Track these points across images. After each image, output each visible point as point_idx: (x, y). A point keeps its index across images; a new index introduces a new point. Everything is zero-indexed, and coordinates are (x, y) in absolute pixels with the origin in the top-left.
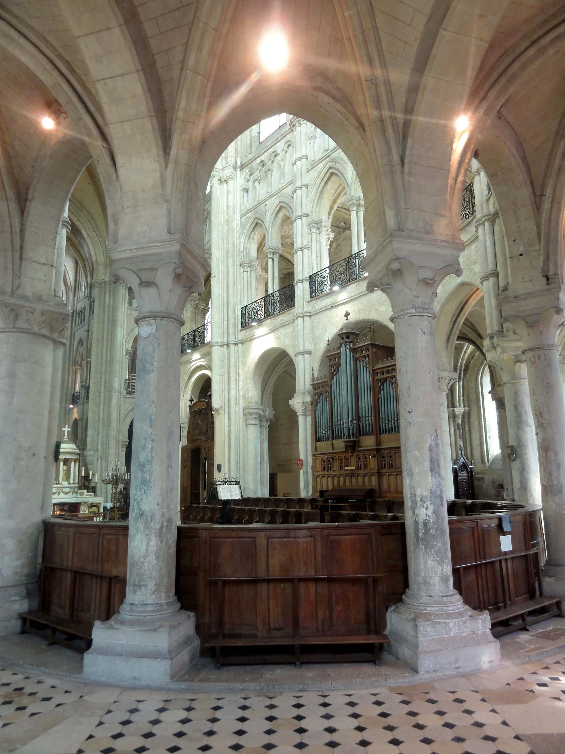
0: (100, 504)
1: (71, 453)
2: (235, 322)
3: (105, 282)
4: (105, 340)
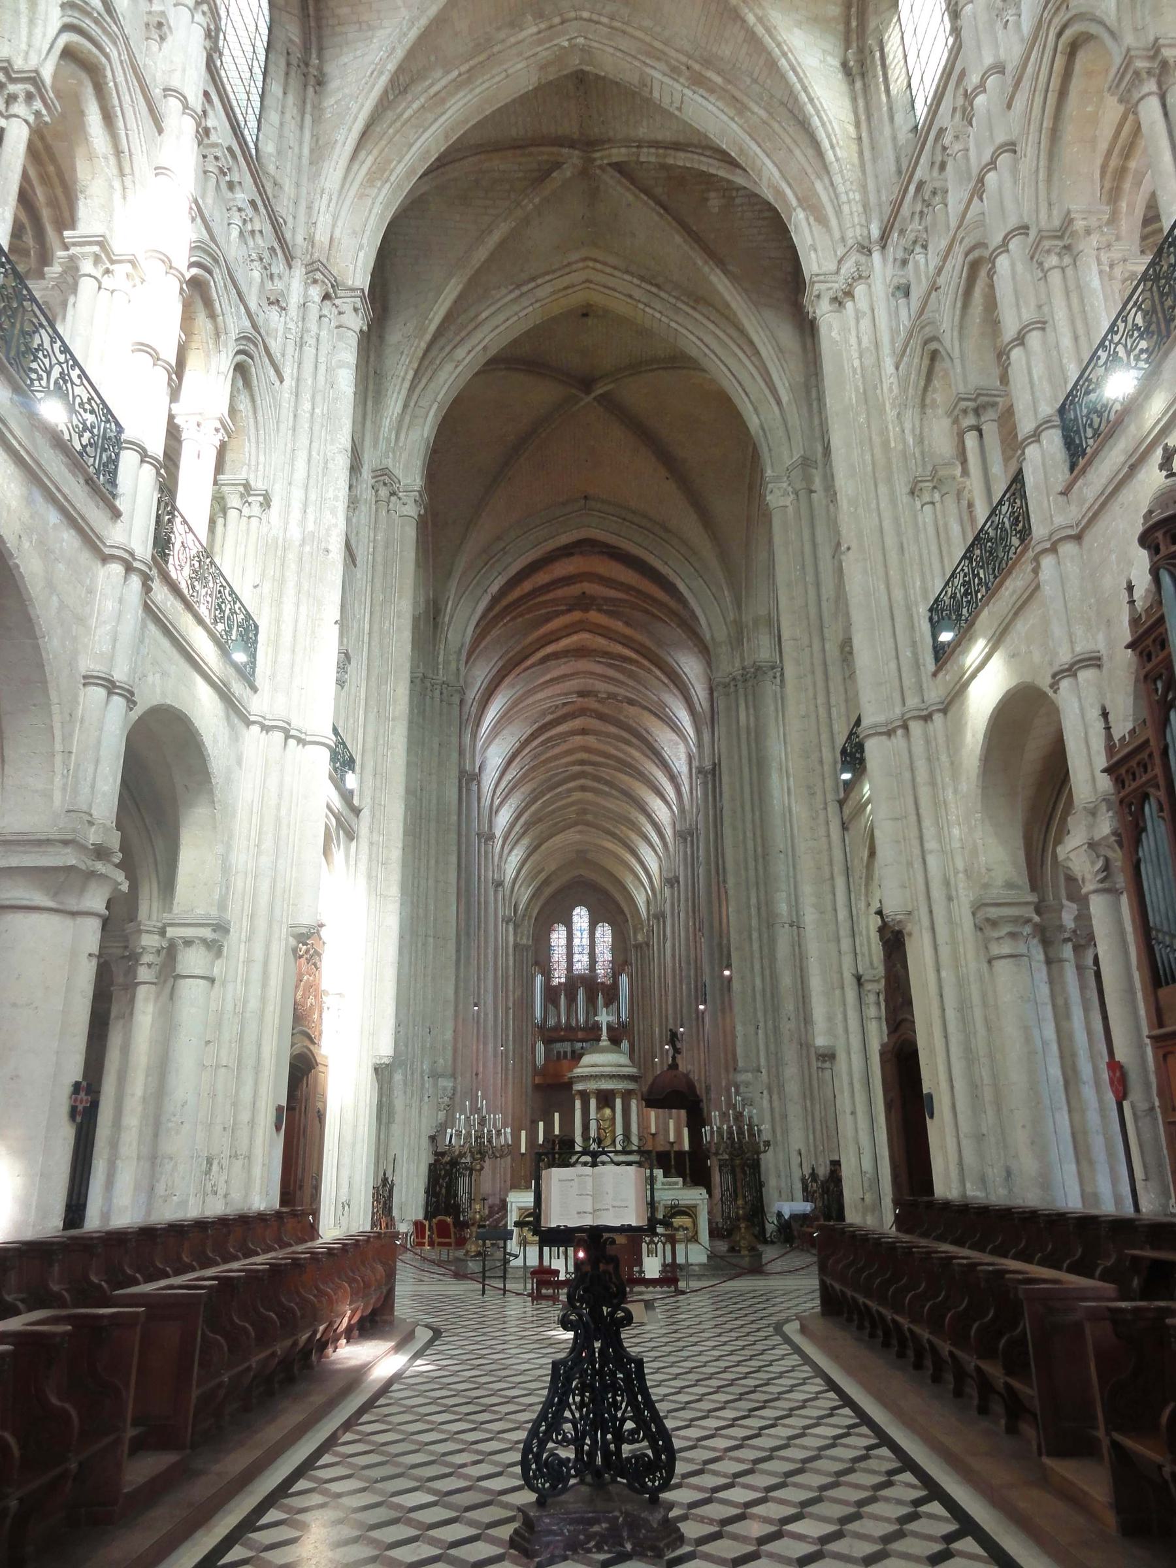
0: (695, 1206)
1: (612, 1077)
2: (915, 654)
3: (734, 679)
4: (748, 807)
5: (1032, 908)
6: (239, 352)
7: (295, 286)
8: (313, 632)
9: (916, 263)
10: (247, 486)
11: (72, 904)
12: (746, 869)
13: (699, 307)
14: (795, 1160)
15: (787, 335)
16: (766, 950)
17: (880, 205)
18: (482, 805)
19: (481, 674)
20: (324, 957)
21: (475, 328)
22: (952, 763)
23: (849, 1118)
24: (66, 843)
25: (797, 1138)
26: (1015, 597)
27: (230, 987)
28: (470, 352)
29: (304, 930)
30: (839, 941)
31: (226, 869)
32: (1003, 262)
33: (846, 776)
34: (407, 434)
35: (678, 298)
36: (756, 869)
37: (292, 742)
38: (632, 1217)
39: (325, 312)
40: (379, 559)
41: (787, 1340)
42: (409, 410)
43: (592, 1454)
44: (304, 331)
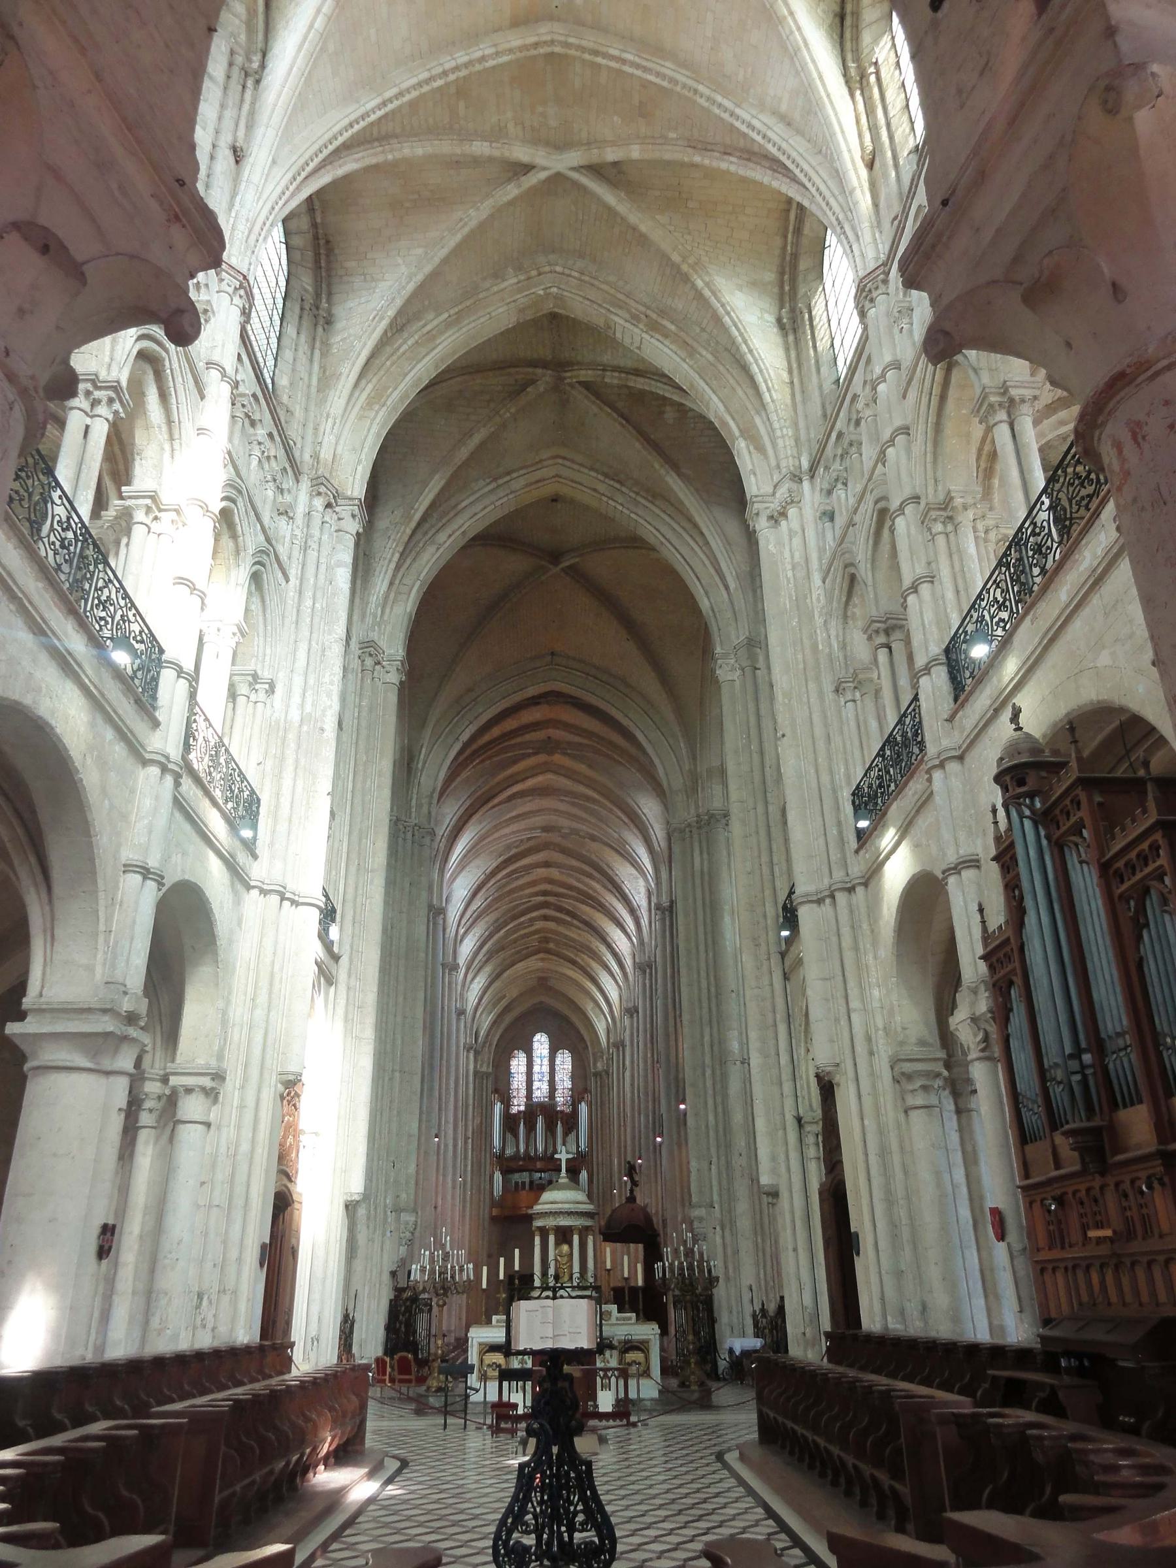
0: (647, 1342)
1: (570, 1214)
2: (840, 833)
3: (689, 825)
4: (702, 948)
5: (941, 1063)
6: (254, 564)
7: (302, 498)
8: (308, 803)
9: (839, 497)
10: (255, 676)
11: (107, 1064)
12: (701, 1008)
13: (657, 503)
14: (746, 1297)
15: (732, 528)
16: (718, 1086)
17: (809, 441)
19: (450, 812)
20: (302, 1098)
21: (456, 515)
22: (872, 931)
23: (791, 1253)
24: (105, 1011)
25: (748, 1275)
26: (917, 797)
27: (225, 1130)
28: (450, 536)
29: (291, 1078)
30: (781, 1085)
31: (224, 1022)
32: (900, 522)
33: (785, 933)
34: (392, 608)
35: (637, 494)
36: (710, 1009)
37: (286, 904)
38: (583, 1341)
39: (327, 519)
40: (364, 723)
41: (726, 1466)
42: (395, 587)
43: (549, 1543)
44: (308, 536)
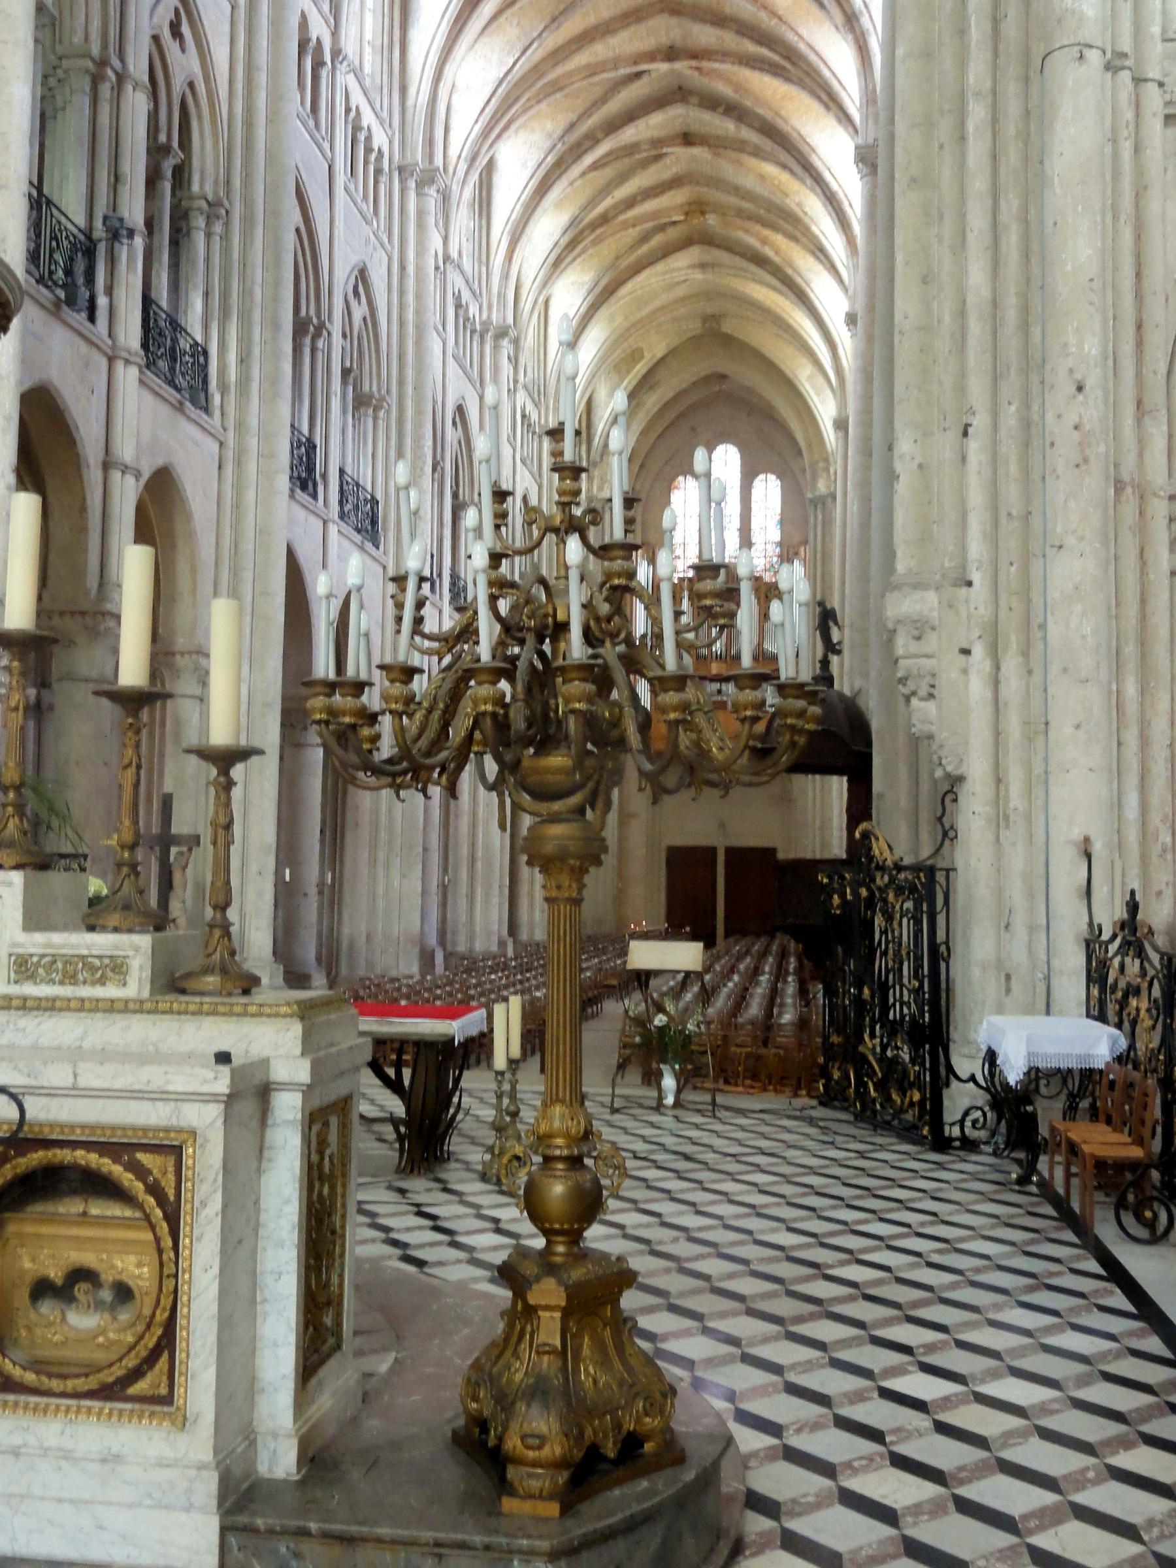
14: (1067, 874)
16: (1012, 157)
18: (410, 102)
